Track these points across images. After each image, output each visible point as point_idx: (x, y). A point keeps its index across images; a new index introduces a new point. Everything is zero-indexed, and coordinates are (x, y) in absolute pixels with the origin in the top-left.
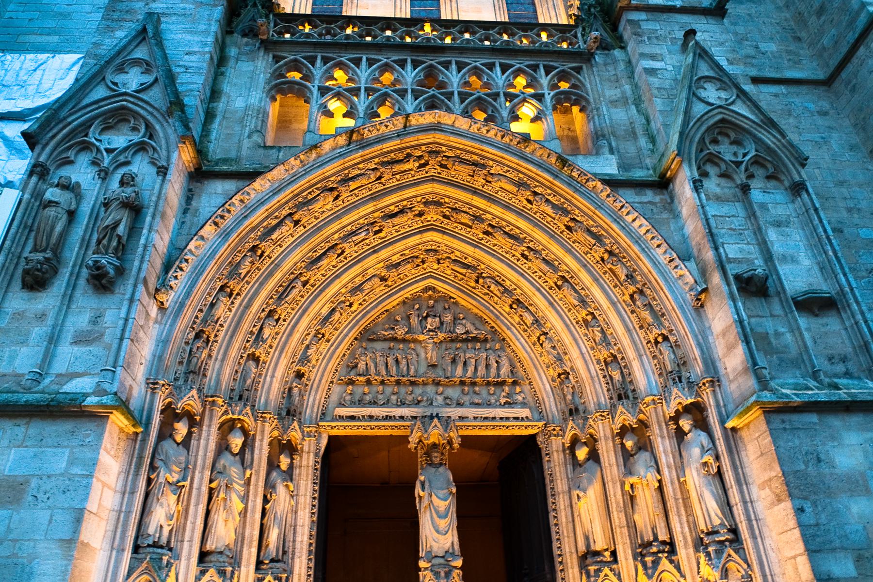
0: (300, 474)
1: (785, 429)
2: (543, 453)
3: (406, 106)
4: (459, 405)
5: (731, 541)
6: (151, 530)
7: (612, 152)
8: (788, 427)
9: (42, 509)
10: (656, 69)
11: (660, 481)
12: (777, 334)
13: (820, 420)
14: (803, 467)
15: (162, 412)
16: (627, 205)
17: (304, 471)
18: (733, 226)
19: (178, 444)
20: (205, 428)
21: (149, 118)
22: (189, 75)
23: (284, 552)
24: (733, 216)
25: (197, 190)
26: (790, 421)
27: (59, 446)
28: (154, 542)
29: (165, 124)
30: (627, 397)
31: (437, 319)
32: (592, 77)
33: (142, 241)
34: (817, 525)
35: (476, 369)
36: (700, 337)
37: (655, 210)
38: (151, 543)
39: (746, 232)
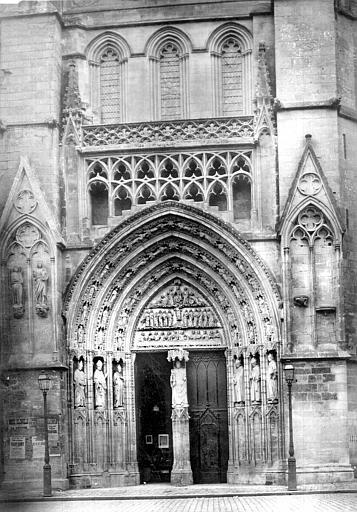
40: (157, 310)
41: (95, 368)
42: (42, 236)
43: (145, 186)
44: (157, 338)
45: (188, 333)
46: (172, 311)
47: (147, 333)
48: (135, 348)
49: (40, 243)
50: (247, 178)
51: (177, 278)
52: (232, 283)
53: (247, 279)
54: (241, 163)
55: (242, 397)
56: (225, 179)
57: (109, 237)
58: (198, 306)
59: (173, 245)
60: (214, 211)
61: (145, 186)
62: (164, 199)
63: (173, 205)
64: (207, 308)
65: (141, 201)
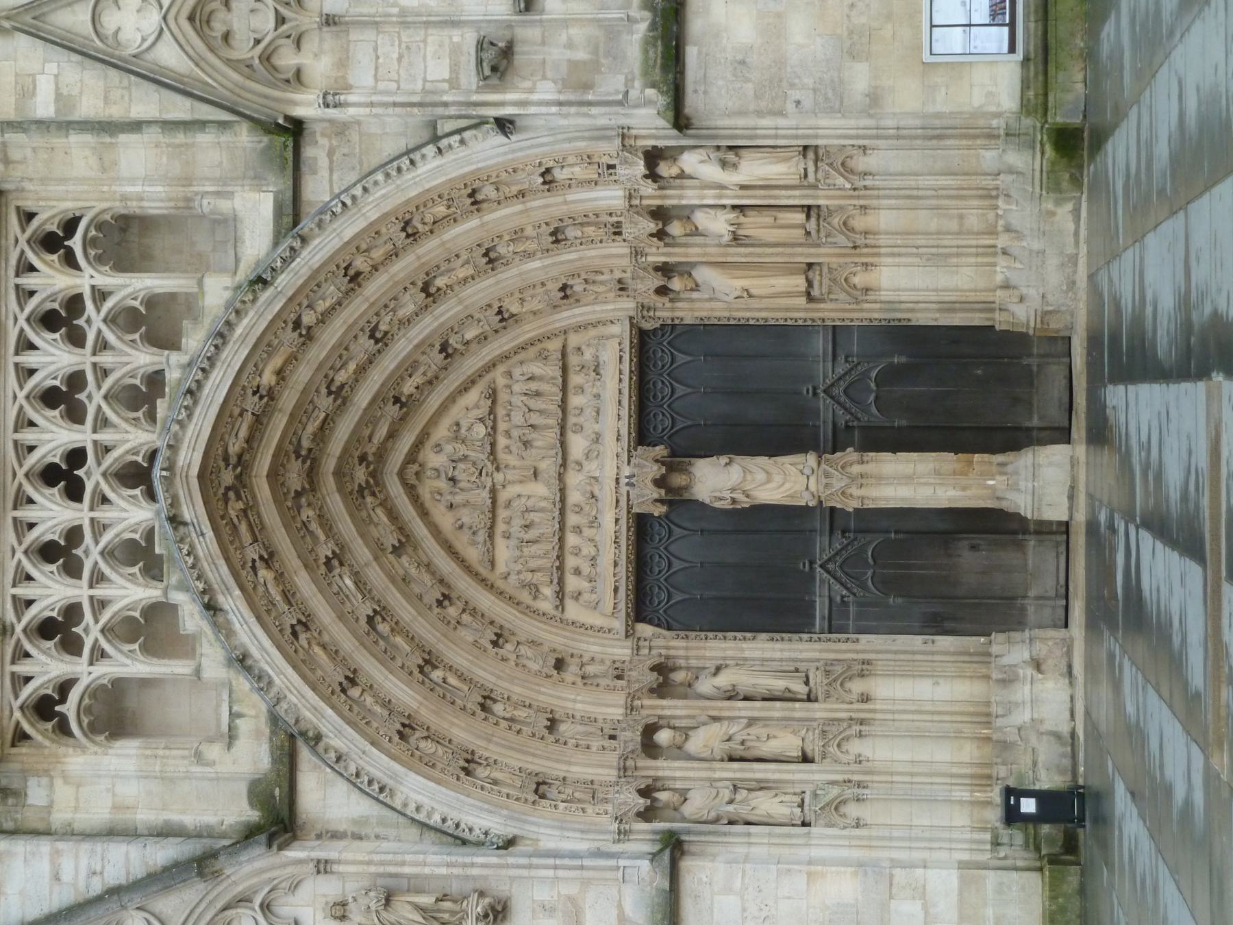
0: (698, 658)
1: (705, 92)
2: (669, 322)
3: (132, 521)
4: (597, 439)
5: (816, 154)
6: (785, 810)
7: (229, 195)
8: (703, 88)
9: (777, 909)
10: (58, 96)
11: (734, 207)
12: (570, 45)
13: (695, 45)
14: (750, 85)
15: (647, 821)
16: (342, 197)
17: (692, 653)
18: (395, 56)
19: (686, 800)
20: (660, 773)
21: (219, 905)
22: (107, 868)
23: (797, 670)
24: (376, 49)
25: (319, 826)
26: (695, 82)
27: (711, 908)
28: (799, 806)
29: (233, 878)
30: (618, 225)
31: (461, 466)
32: (43, 194)
33: (443, 871)
34: (814, 90)
35: (541, 412)
36: (560, 137)
37: (346, 151)
38: (800, 810)
39: (404, 39)
40: (500, 543)
41: (679, 751)
42: (243, 900)
43: (107, 554)
44: (588, 550)
45: (578, 445)
46: (503, 496)
47: (572, 583)
48: (619, 624)
49: (266, 907)
50: (100, 226)
51: (401, 474)
52: (425, 289)
53: (413, 236)
54: (51, 243)
55: (788, 269)
56: (100, 295)
57: (262, 681)
58: (492, 411)
59: (294, 477)
60: (194, 340)
61: (107, 554)
62: (151, 496)
63: (170, 468)
64: (501, 382)
65: (153, 568)
